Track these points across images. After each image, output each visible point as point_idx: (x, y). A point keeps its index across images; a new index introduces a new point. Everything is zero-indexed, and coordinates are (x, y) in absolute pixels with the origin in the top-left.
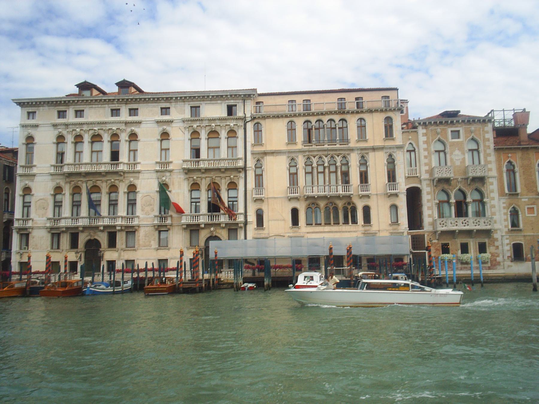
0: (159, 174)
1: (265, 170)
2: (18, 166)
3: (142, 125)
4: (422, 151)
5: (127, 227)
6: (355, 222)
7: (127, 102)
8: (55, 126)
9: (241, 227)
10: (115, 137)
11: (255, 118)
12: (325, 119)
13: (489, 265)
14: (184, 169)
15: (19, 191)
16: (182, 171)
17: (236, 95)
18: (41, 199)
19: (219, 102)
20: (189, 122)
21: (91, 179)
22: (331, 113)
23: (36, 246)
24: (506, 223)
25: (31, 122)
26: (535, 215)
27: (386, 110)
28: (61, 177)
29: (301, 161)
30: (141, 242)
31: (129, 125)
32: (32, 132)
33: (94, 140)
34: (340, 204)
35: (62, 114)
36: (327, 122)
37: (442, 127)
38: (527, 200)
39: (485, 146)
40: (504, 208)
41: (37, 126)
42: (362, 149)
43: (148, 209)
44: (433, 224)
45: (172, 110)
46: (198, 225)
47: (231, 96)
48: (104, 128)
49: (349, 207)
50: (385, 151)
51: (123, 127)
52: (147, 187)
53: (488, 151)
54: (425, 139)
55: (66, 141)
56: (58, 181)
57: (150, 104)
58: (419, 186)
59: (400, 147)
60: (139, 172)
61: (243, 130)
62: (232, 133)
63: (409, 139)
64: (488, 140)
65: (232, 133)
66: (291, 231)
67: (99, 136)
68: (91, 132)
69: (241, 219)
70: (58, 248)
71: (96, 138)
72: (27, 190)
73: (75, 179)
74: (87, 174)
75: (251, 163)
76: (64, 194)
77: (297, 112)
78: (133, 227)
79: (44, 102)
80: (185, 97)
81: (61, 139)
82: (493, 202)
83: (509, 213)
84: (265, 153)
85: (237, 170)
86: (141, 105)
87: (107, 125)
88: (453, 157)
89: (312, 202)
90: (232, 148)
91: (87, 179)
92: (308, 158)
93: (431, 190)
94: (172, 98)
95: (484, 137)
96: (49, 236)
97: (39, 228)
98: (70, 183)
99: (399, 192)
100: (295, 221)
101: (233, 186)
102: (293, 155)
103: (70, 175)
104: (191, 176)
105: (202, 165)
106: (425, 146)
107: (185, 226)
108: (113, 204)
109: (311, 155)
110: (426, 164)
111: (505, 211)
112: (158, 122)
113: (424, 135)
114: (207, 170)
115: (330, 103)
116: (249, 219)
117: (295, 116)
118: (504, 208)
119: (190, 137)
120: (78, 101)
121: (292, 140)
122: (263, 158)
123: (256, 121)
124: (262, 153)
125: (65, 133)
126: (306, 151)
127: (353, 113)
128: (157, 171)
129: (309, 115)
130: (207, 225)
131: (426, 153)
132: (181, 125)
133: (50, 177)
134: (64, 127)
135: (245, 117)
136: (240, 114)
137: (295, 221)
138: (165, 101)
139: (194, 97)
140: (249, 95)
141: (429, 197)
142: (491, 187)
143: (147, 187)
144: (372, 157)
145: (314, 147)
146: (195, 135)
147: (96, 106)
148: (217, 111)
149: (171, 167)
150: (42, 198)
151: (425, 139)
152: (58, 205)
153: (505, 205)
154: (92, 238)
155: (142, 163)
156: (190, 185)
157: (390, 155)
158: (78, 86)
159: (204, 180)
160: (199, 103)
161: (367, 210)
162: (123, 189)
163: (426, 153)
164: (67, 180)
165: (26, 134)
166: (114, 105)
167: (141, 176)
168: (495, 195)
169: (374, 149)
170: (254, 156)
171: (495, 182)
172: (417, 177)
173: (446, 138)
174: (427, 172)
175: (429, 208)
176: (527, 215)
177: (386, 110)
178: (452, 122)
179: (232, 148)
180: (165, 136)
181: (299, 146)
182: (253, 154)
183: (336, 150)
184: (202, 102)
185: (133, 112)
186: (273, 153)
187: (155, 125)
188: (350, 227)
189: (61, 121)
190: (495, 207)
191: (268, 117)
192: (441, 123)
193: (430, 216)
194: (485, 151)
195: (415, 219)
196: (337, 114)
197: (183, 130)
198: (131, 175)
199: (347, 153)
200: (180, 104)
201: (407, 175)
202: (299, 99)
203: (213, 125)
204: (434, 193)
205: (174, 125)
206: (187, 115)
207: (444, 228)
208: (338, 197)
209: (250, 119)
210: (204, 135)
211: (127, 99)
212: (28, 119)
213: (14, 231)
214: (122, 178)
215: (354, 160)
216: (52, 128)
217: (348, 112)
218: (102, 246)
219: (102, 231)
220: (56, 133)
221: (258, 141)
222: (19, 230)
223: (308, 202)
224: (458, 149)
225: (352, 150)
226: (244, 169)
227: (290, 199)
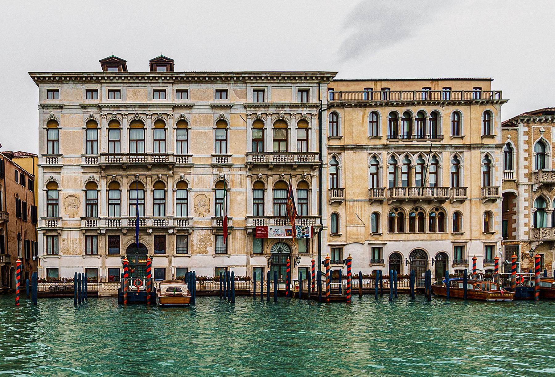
0: (216, 170)
1: (343, 168)
4: (521, 151)
6: (442, 229)
10: (160, 124)
16: (244, 166)
18: (71, 196)
20: (252, 109)
21: (133, 173)
28: (95, 170)
29: (385, 158)
31: (177, 109)
32: (57, 114)
33: (133, 126)
36: (416, 113)
37: (546, 125)
42: (456, 148)
43: (202, 209)
45: (231, 92)
48: (147, 113)
50: (482, 150)
51: (170, 111)
55: (99, 127)
56: (91, 175)
58: (515, 191)
59: (499, 146)
60: (191, 167)
61: (318, 120)
63: (508, 138)
67: (141, 122)
72: (52, 185)
76: (100, 191)
81: (92, 124)
84: (344, 148)
85: (311, 167)
87: (149, 109)
91: (128, 173)
93: (529, 197)
103: (106, 168)
104: (255, 173)
106: (526, 147)
109: (397, 153)
110: (525, 167)
112: (214, 107)
122: (339, 154)
123: (332, 110)
124: (339, 148)
126: (392, 148)
128: (213, 166)
131: (526, 155)
132: (243, 111)
133: (81, 170)
136: (314, 100)
141: (527, 204)
144: (466, 157)
145: (401, 142)
146: (259, 124)
148: (287, 95)
150: (71, 194)
152: (92, 204)
155: (194, 155)
156: (253, 183)
157: (487, 156)
159: (270, 179)
160: (263, 85)
163: (526, 155)
164: (103, 173)
165: (47, 116)
166: (158, 85)
167: (192, 170)
172: (514, 181)
174: (526, 176)
180: (222, 124)
182: (330, 148)
184: (268, 85)
187: (210, 111)
198: (181, 170)
199: (439, 151)
200: (241, 86)
205: (233, 111)
210: (269, 124)
214: (171, 172)
220: (87, 116)
225: (444, 147)
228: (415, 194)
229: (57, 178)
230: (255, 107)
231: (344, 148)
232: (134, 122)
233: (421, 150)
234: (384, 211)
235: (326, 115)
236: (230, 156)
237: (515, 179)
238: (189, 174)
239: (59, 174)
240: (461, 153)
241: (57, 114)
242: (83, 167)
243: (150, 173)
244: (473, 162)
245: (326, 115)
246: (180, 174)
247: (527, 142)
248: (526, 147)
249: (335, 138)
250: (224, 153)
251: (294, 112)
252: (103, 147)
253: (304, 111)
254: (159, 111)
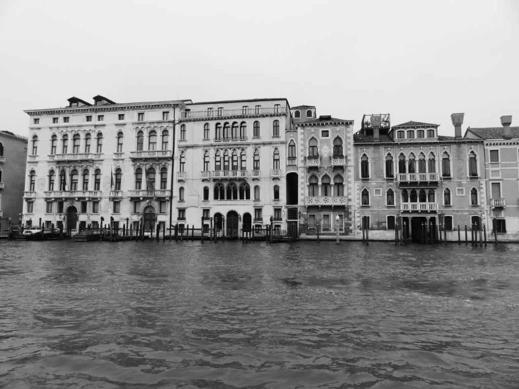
0: (116, 161)
2: (28, 156)
3: (106, 127)
4: (299, 145)
5: (93, 198)
6: (248, 197)
7: (96, 111)
8: (51, 128)
9: (168, 200)
10: (88, 135)
11: (181, 121)
12: (231, 122)
13: (344, 232)
14: (131, 158)
15: (28, 173)
17: (168, 105)
19: (157, 110)
20: (137, 125)
22: (234, 117)
23: (38, 210)
24: (358, 201)
25: (37, 126)
26: (381, 195)
27: (274, 115)
29: (212, 152)
30: (102, 209)
34: (238, 184)
35: (55, 120)
36: (230, 124)
37: (315, 128)
38: (375, 184)
39: (346, 142)
40: (358, 189)
41: (40, 129)
42: (256, 144)
44: (304, 200)
45: (126, 117)
46: (139, 198)
47: (165, 105)
48: (81, 129)
49: (245, 187)
51: (93, 128)
52: (107, 171)
53: (349, 146)
54: (302, 136)
58: (296, 172)
62: (165, 133)
63: (291, 137)
64: (350, 138)
65: (165, 133)
66: (202, 203)
68: (74, 132)
69: (168, 194)
70: (51, 212)
71: (76, 137)
73: (62, 165)
74: (69, 162)
75: (177, 154)
77: (211, 117)
78: (97, 198)
79: (44, 112)
80: (134, 107)
81: (54, 137)
82: (349, 185)
83: (361, 194)
84: (188, 147)
88: (322, 151)
89: (218, 183)
90: (165, 143)
92: (217, 151)
94: (125, 108)
95: (346, 135)
96: (46, 203)
97: (40, 198)
98: (59, 168)
99: (280, 177)
100: (206, 197)
101: (164, 171)
102: (206, 148)
103: (58, 162)
105: (143, 156)
106: (302, 142)
107: (130, 199)
108: (85, 182)
111: (358, 192)
112: (117, 125)
113: (303, 134)
114: (146, 159)
115: (237, 109)
116: (174, 194)
117: (209, 119)
118: (358, 189)
119: (137, 135)
120: (65, 111)
121: (206, 138)
122: (185, 150)
123: (182, 123)
125: (57, 133)
127: (250, 117)
128: (114, 160)
129: (219, 119)
130: (145, 199)
133: (48, 164)
134: (56, 129)
135: (174, 121)
136: (171, 118)
137: (206, 197)
138: (121, 109)
139: (140, 107)
140: (177, 105)
142: (349, 174)
143: (107, 171)
145: (222, 142)
147: (77, 114)
149: (122, 157)
150: (41, 177)
151: (302, 136)
152: (51, 182)
153: (358, 187)
154: (71, 206)
155: (105, 153)
158: (69, 100)
160: (143, 111)
161: (257, 188)
162: (92, 172)
163: (302, 148)
164: (57, 166)
167: (103, 162)
168: (352, 179)
169: (264, 144)
170: (180, 149)
171: (352, 169)
173: (318, 136)
175: (302, 189)
176: (375, 195)
177: (274, 115)
178: (323, 124)
179: (165, 143)
180: (120, 135)
181: (212, 142)
183: (237, 145)
185: (100, 117)
186: (192, 147)
188: (245, 201)
189: (56, 125)
190: (351, 189)
191: (190, 121)
192: (314, 125)
193: (302, 194)
194: (346, 146)
195: (292, 196)
196: (239, 118)
197: (132, 130)
198: (97, 162)
201: (288, 164)
202: (215, 107)
203: (152, 126)
204: (307, 178)
206: (136, 119)
207: (311, 204)
208: (235, 179)
209: (178, 122)
211: (96, 109)
212: (35, 123)
213: (24, 200)
215: (250, 151)
216: (49, 129)
217: (247, 117)
218: (78, 211)
219: (78, 201)
221: (183, 139)
222: (27, 199)
223: (215, 183)
224: (327, 145)
225: (249, 145)
226: (172, 158)
227: (203, 180)
228: (230, 175)
229: (35, 169)
230: (138, 124)
231: (188, 147)
232: (75, 135)
233: (234, 146)
234: (211, 187)
235: (178, 127)
236: (123, 153)
237: (296, 164)
238: (102, 164)
239: (36, 166)
240: (259, 147)
241: (37, 132)
242: (48, 162)
243: (81, 165)
244: (266, 154)
245: (178, 127)
246: (97, 165)
247: (303, 139)
248: (302, 142)
249: (183, 141)
250: (120, 152)
251: (159, 125)
252: (59, 150)
253: (165, 125)
254: (87, 129)
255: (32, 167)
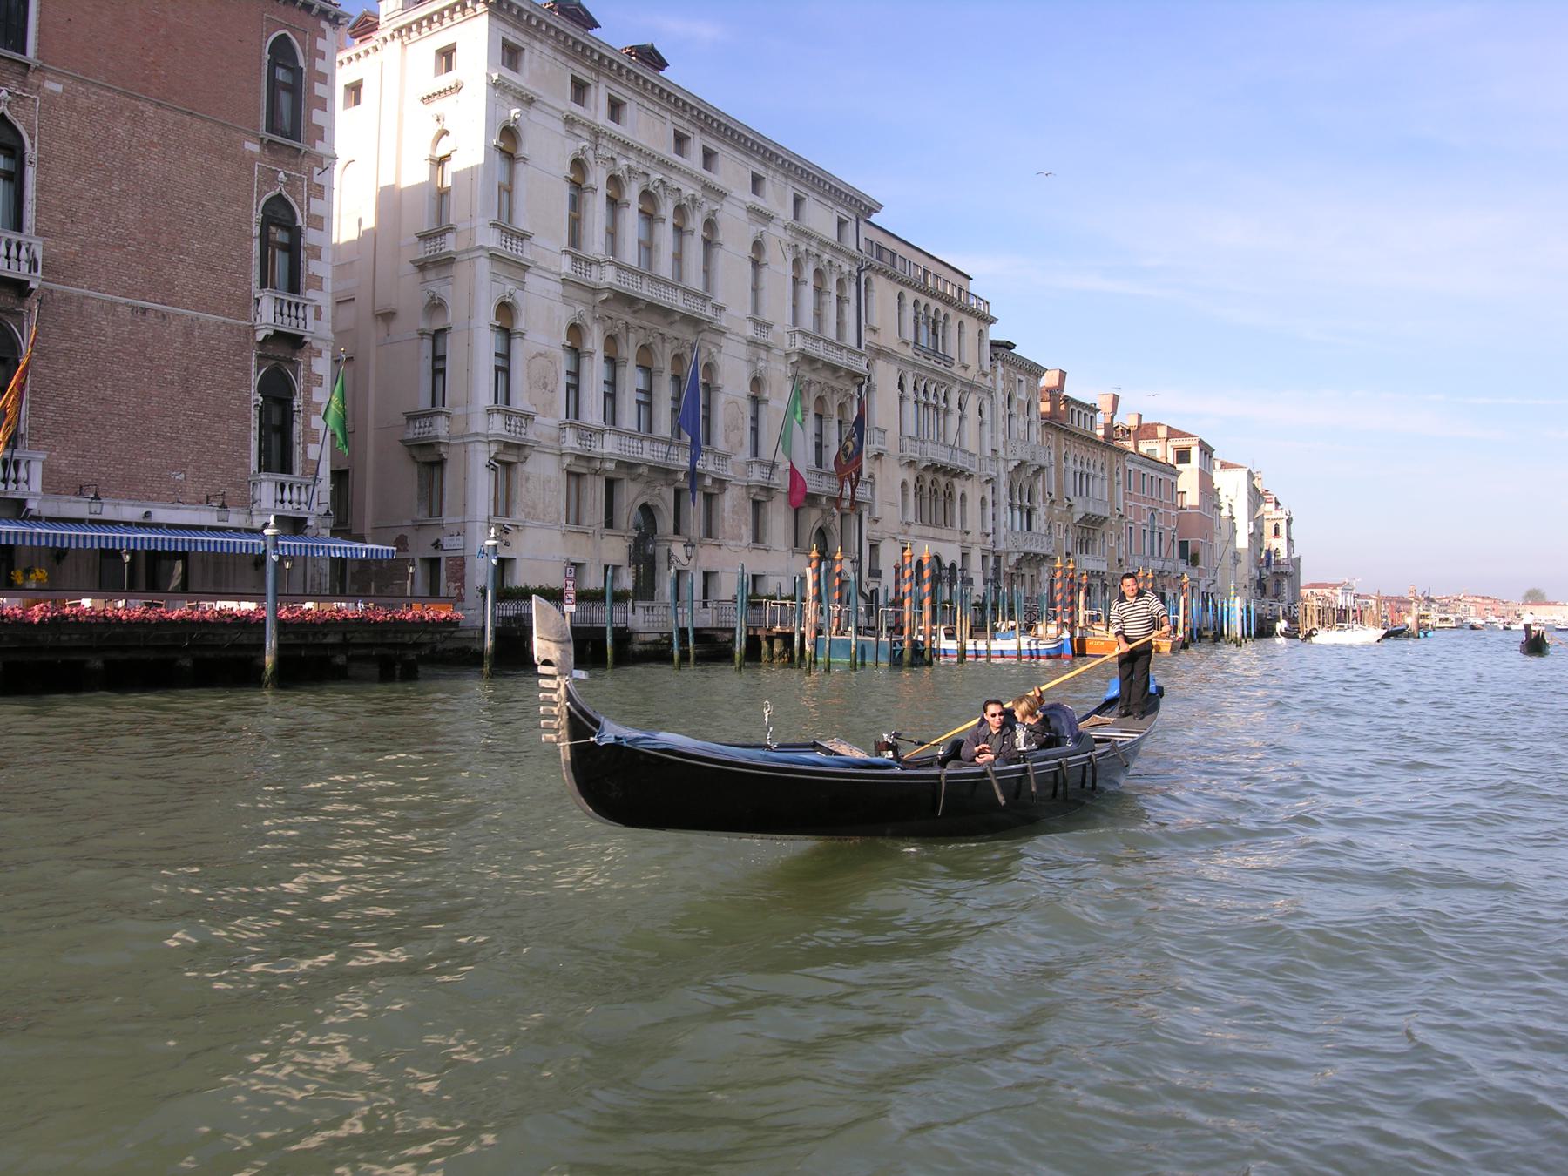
21: (646, 324)
57: (737, 154)
86: (724, 147)
102: (904, 368)
133: (559, 288)
147: (651, 107)
150: (542, 349)
187: (743, 215)
216: (560, 127)
255: (510, 287)
